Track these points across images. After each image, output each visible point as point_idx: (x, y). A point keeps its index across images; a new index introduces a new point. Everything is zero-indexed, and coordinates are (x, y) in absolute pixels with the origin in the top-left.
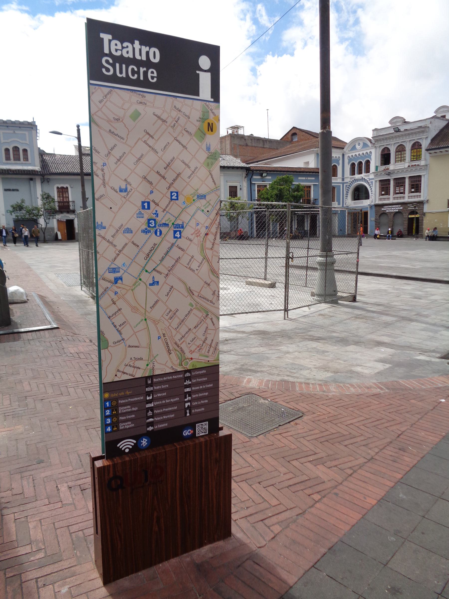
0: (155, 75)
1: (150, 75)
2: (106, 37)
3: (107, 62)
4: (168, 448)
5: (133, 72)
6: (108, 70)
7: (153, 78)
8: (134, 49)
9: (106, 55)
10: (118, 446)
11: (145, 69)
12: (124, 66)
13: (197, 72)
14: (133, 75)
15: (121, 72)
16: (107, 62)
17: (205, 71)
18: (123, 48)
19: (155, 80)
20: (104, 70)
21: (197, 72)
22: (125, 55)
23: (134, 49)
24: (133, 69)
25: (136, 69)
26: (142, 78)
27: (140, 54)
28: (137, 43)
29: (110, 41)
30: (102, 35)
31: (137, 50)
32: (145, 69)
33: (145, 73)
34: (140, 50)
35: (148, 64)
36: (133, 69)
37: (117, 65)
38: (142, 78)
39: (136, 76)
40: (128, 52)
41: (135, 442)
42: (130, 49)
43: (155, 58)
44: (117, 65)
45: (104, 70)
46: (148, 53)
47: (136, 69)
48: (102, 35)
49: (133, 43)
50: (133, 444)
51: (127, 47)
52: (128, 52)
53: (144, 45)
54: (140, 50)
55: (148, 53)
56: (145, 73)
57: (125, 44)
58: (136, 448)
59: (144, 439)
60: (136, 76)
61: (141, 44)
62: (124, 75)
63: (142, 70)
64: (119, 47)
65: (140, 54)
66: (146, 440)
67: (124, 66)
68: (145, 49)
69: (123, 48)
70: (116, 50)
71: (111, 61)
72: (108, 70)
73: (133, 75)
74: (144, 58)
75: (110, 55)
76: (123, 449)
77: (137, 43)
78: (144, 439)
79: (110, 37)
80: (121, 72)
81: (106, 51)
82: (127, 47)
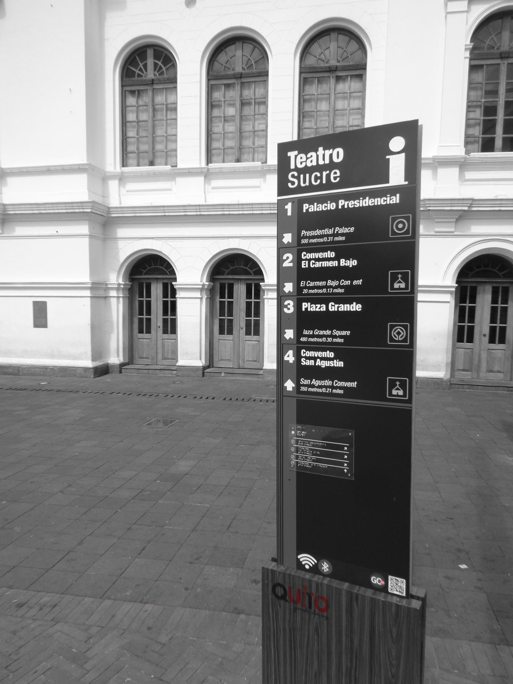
0: (338, 174)
1: (332, 176)
2: (292, 154)
3: (293, 176)
4: (346, 586)
5: (316, 178)
6: (293, 183)
7: (335, 178)
8: (317, 156)
9: (293, 170)
10: (299, 557)
11: (328, 172)
12: (308, 175)
13: (387, 157)
14: (316, 181)
15: (305, 182)
16: (293, 176)
17: (399, 153)
18: (307, 158)
19: (338, 179)
20: (290, 185)
21: (387, 157)
22: (309, 164)
23: (317, 156)
24: (316, 176)
25: (319, 175)
26: (324, 182)
27: (324, 159)
28: (321, 149)
29: (296, 156)
30: (289, 154)
31: (322, 156)
32: (328, 172)
33: (328, 176)
34: (324, 155)
35: (332, 166)
36: (316, 176)
37: (302, 176)
38: (324, 182)
39: (319, 181)
40: (311, 161)
41: (316, 562)
42: (314, 159)
43: (338, 157)
44: (302, 176)
45: (290, 185)
46: (331, 156)
47: (319, 175)
48: (289, 154)
49: (316, 151)
50: (314, 563)
51: (311, 156)
52: (311, 161)
53: (327, 149)
54: (324, 155)
55: (331, 156)
56: (328, 176)
57: (309, 156)
58: (315, 570)
59: (325, 563)
60: (319, 181)
61: (324, 150)
62: (307, 184)
63: (325, 174)
64: (304, 159)
65: (324, 159)
66: (328, 566)
67: (308, 175)
68: (328, 153)
69: (307, 158)
70: (301, 163)
71: (296, 174)
72: (293, 183)
73: (316, 181)
74: (327, 161)
75: (296, 169)
76: (303, 563)
77: (321, 149)
78: (325, 563)
79: (296, 153)
80: (305, 182)
81: (292, 167)
82: (311, 156)
